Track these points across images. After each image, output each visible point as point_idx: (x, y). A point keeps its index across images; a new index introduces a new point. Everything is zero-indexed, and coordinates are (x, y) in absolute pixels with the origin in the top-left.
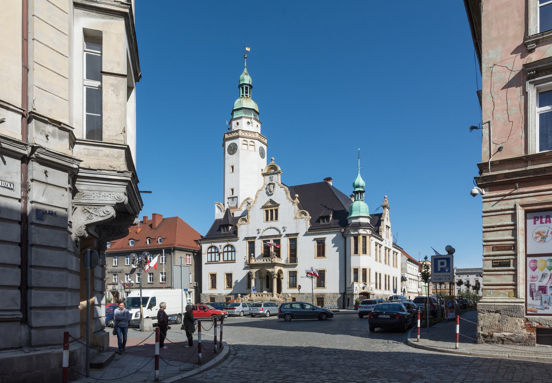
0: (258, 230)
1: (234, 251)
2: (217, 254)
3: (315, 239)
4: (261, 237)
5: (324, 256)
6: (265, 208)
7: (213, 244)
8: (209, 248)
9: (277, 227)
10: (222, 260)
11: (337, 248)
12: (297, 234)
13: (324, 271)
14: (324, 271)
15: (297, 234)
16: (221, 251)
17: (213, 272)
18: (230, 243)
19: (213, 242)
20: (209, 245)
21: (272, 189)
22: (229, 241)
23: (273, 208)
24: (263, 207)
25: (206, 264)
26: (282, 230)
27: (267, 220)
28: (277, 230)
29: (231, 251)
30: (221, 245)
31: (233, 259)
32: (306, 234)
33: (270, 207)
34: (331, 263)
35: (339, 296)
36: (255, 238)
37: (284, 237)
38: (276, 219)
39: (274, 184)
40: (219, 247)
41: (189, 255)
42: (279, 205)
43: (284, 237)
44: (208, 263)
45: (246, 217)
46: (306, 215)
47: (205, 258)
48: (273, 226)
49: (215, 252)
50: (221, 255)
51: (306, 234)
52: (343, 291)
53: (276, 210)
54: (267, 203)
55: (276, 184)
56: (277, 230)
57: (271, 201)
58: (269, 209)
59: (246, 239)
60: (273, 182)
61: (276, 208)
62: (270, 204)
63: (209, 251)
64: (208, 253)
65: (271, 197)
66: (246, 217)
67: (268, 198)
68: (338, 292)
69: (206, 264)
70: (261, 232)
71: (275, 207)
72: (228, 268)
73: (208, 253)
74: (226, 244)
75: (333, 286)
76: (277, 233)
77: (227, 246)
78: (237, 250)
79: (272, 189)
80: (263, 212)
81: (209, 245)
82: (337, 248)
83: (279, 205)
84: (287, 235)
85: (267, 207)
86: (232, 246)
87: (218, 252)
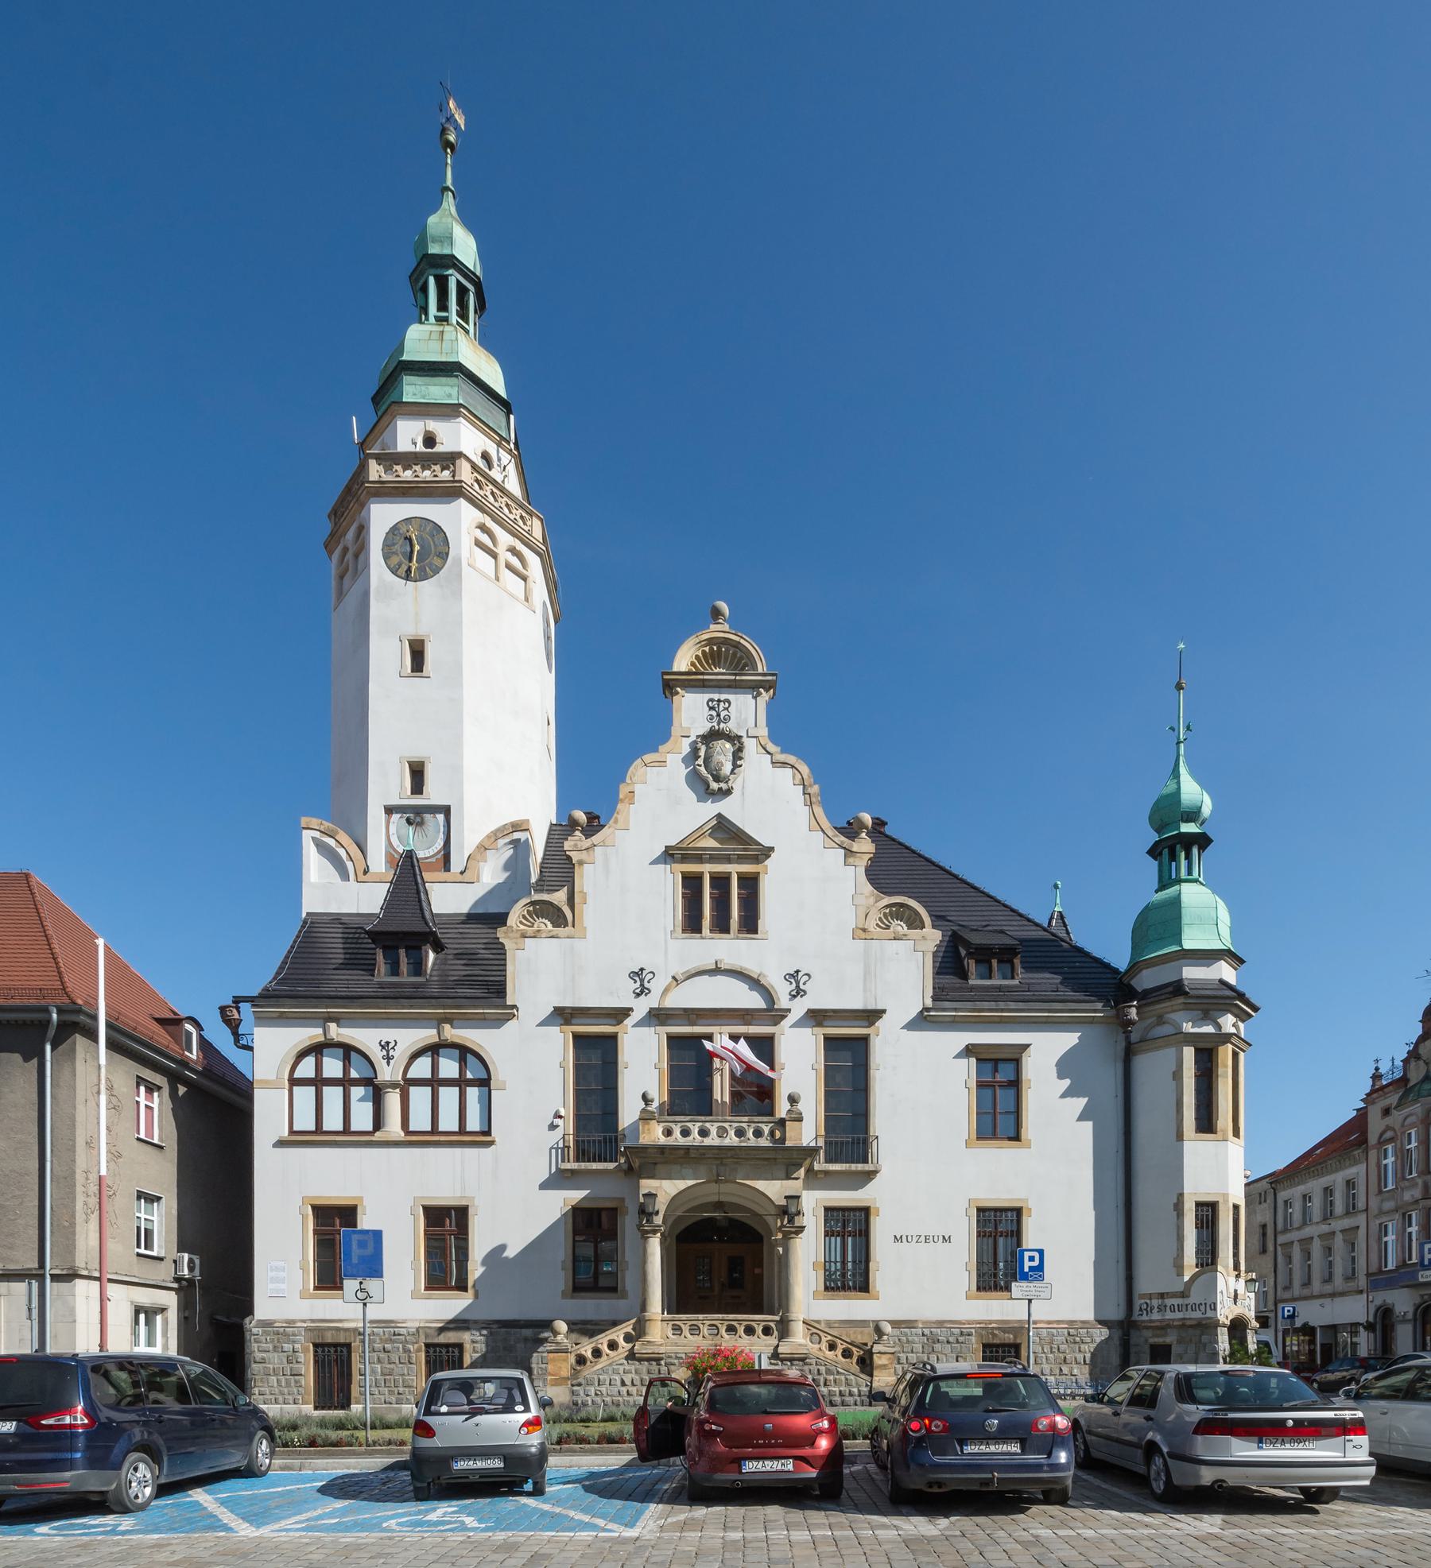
0: (638, 974)
1: (485, 1083)
2: (357, 1092)
3: (969, 1051)
4: (658, 1016)
5: (1016, 1137)
7: (336, 1032)
8: (302, 1055)
9: (753, 969)
10: (393, 1127)
11: (1081, 1102)
12: (872, 1016)
13: (1018, 1211)
14: (1018, 1211)
15: (872, 1016)
16: (387, 1073)
18: (451, 1033)
19: (337, 1019)
21: (727, 768)
22: (449, 1020)
23: (734, 869)
24: (670, 855)
25: (281, 1143)
27: (692, 924)
28: (755, 983)
29: (461, 1083)
30: (392, 1043)
31: (474, 1123)
32: (923, 1021)
33: (714, 859)
34: (1055, 1172)
35: (1101, 1334)
37: (798, 1024)
38: (750, 924)
39: (734, 739)
41: (151, 1089)
42: (767, 852)
43: (798, 1024)
44: (295, 1140)
45: (559, 897)
46: (914, 922)
47: (270, 1114)
49: (345, 1083)
50: (393, 1100)
51: (923, 1021)
52: (1116, 1313)
54: (698, 833)
55: (750, 745)
56: (755, 983)
57: (723, 827)
58: (707, 869)
59: (563, 1015)
60: (732, 726)
62: (711, 843)
63: (307, 1069)
64: (294, 1082)
65: (725, 807)
66: (559, 897)
67: (708, 811)
68: (1089, 1315)
69: (281, 1143)
70: (657, 986)
71: (741, 859)
72: (444, 1175)
73: (294, 1082)
74: (426, 1035)
75: (1066, 1294)
76: (755, 1001)
77: (433, 1050)
78: (500, 1072)
79: (727, 768)
80: (668, 884)
82: (1081, 1102)
83: (767, 852)
84: (816, 1017)
85: (699, 858)
86: (464, 1053)
87: (367, 1082)
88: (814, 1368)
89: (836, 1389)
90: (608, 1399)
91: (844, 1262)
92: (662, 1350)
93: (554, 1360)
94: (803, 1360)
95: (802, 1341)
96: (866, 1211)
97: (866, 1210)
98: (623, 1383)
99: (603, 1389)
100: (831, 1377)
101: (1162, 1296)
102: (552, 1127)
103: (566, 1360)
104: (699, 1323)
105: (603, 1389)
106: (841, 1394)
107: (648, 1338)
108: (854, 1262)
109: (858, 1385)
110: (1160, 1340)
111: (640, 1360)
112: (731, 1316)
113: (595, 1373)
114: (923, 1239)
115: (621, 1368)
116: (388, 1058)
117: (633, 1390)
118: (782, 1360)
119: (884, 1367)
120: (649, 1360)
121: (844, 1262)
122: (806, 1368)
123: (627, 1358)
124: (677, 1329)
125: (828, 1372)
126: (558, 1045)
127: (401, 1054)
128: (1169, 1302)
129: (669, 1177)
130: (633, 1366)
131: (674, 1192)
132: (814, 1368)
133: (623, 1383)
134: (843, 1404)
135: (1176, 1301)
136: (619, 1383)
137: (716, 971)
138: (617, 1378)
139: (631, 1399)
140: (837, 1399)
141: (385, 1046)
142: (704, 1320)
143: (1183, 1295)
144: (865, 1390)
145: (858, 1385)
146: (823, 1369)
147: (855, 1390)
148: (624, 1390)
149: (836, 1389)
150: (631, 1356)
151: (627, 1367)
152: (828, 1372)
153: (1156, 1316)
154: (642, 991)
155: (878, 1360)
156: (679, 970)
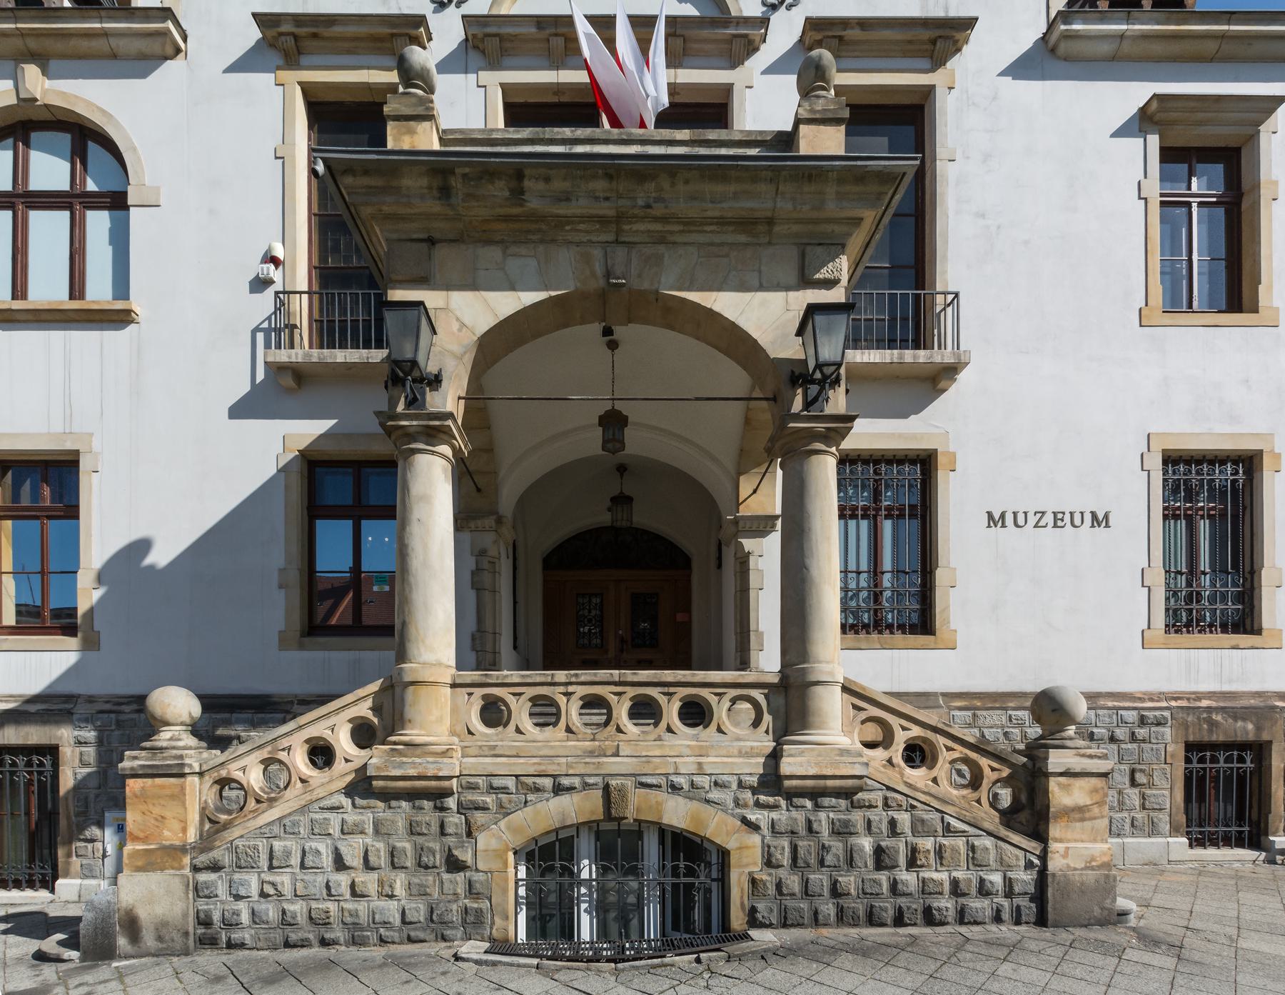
88: (879, 817)
89: (943, 876)
90: (297, 908)
91: (876, 571)
92: (451, 766)
93: (143, 796)
94: (847, 794)
95: (844, 741)
96: (924, 464)
97: (924, 464)
98: (340, 864)
99: (284, 880)
100: (927, 844)
102: (260, 284)
103: (179, 797)
104: (556, 693)
105: (284, 880)
106: (956, 889)
107: (412, 734)
108: (898, 572)
109: (1004, 866)
111: (387, 796)
112: (644, 675)
113: (261, 833)
114: (1049, 518)
115: (335, 820)
117: (369, 881)
118: (790, 795)
119: (1079, 813)
120: (412, 796)
121: (876, 571)
122: (857, 817)
123: (350, 791)
124: (494, 713)
125: (920, 827)
126: (271, 118)
129: (471, 284)
130: (366, 815)
131: (484, 323)
132: (879, 817)
133: (340, 864)
134: (962, 917)
136: (327, 860)
138: (323, 847)
139: (361, 907)
140: (945, 904)
142: (570, 687)
144: (1024, 878)
145: (1004, 866)
146: (904, 818)
147: (996, 878)
148: (343, 880)
149: (943, 876)
150: (361, 786)
151: (352, 817)
152: (920, 827)
155: (1061, 795)
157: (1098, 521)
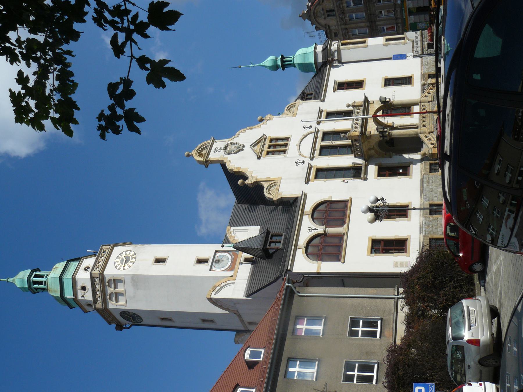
6: (261, 153)
17: (366, 245)
20: (300, 254)
24: (259, 158)
26: (309, 130)
28: (306, 136)
36: (310, 167)
40: (313, 233)
48: (298, 142)
53: (271, 140)
57: (254, 145)
59: (307, 182)
61: (267, 141)
66: (265, 185)
67: (247, 149)
76: (311, 137)
81: (300, 254)
101: (413, 47)
110: (426, 47)
116: (315, 229)
127: (313, 225)
128: (415, 45)
135: (415, 43)
137: (300, 146)
141: (310, 230)
143: (413, 42)
153: (419, 49)
154: (303, 162)
156: (297, 153)
157: (394, 91)
